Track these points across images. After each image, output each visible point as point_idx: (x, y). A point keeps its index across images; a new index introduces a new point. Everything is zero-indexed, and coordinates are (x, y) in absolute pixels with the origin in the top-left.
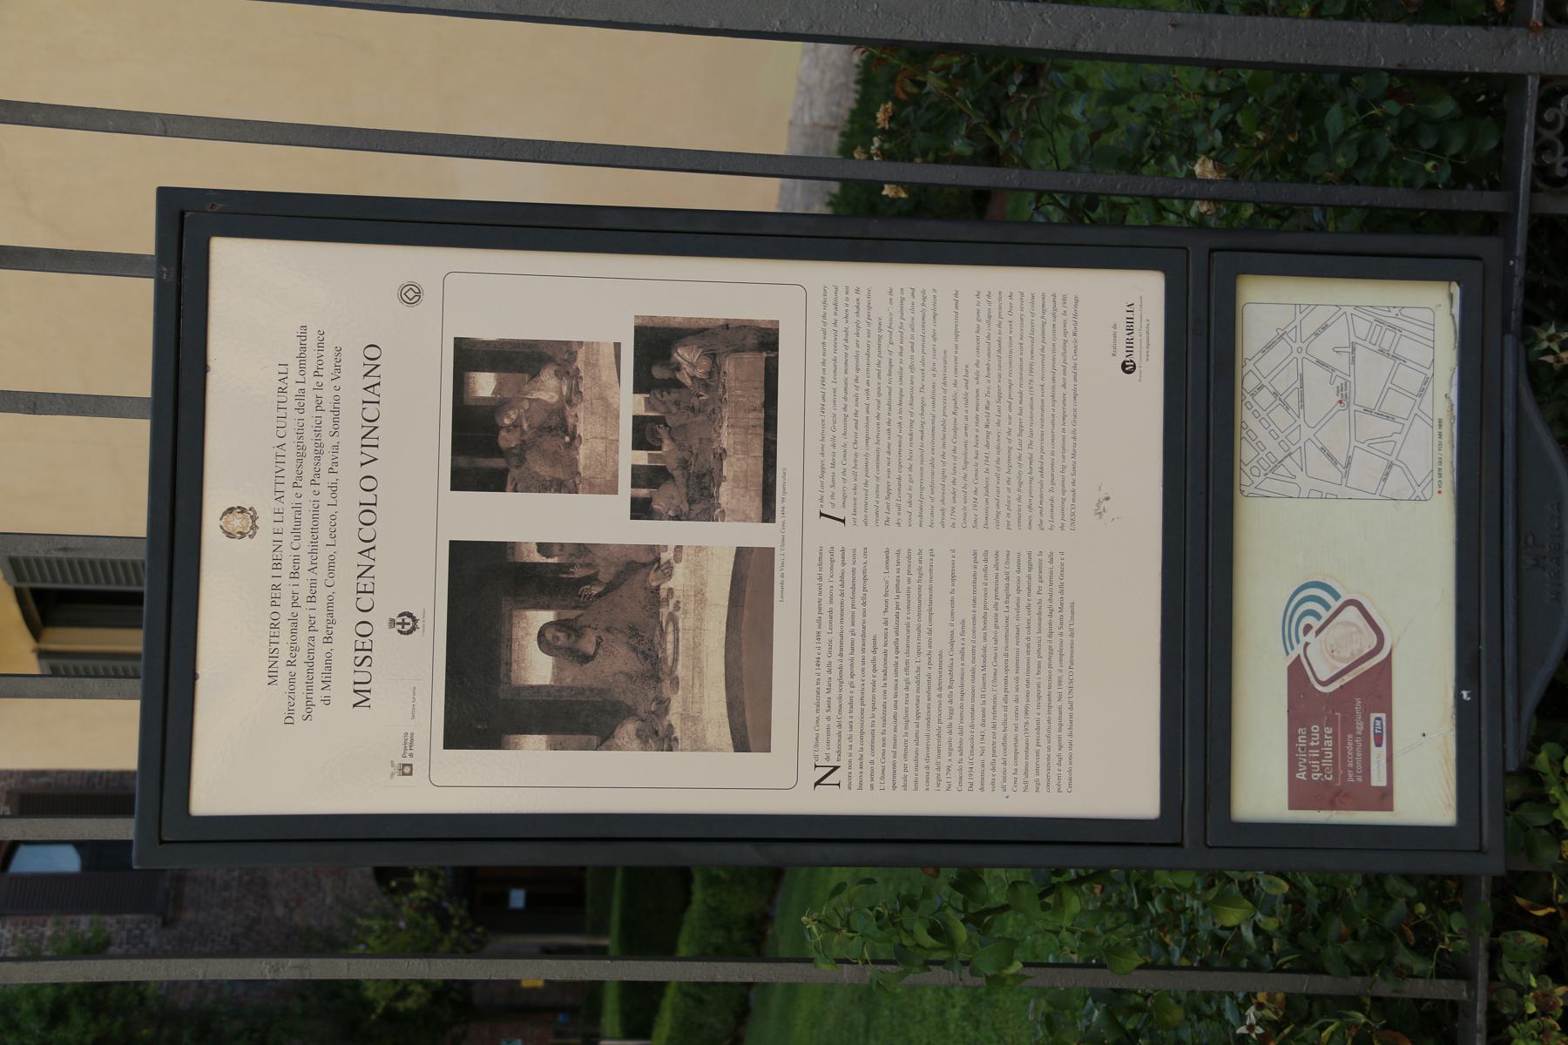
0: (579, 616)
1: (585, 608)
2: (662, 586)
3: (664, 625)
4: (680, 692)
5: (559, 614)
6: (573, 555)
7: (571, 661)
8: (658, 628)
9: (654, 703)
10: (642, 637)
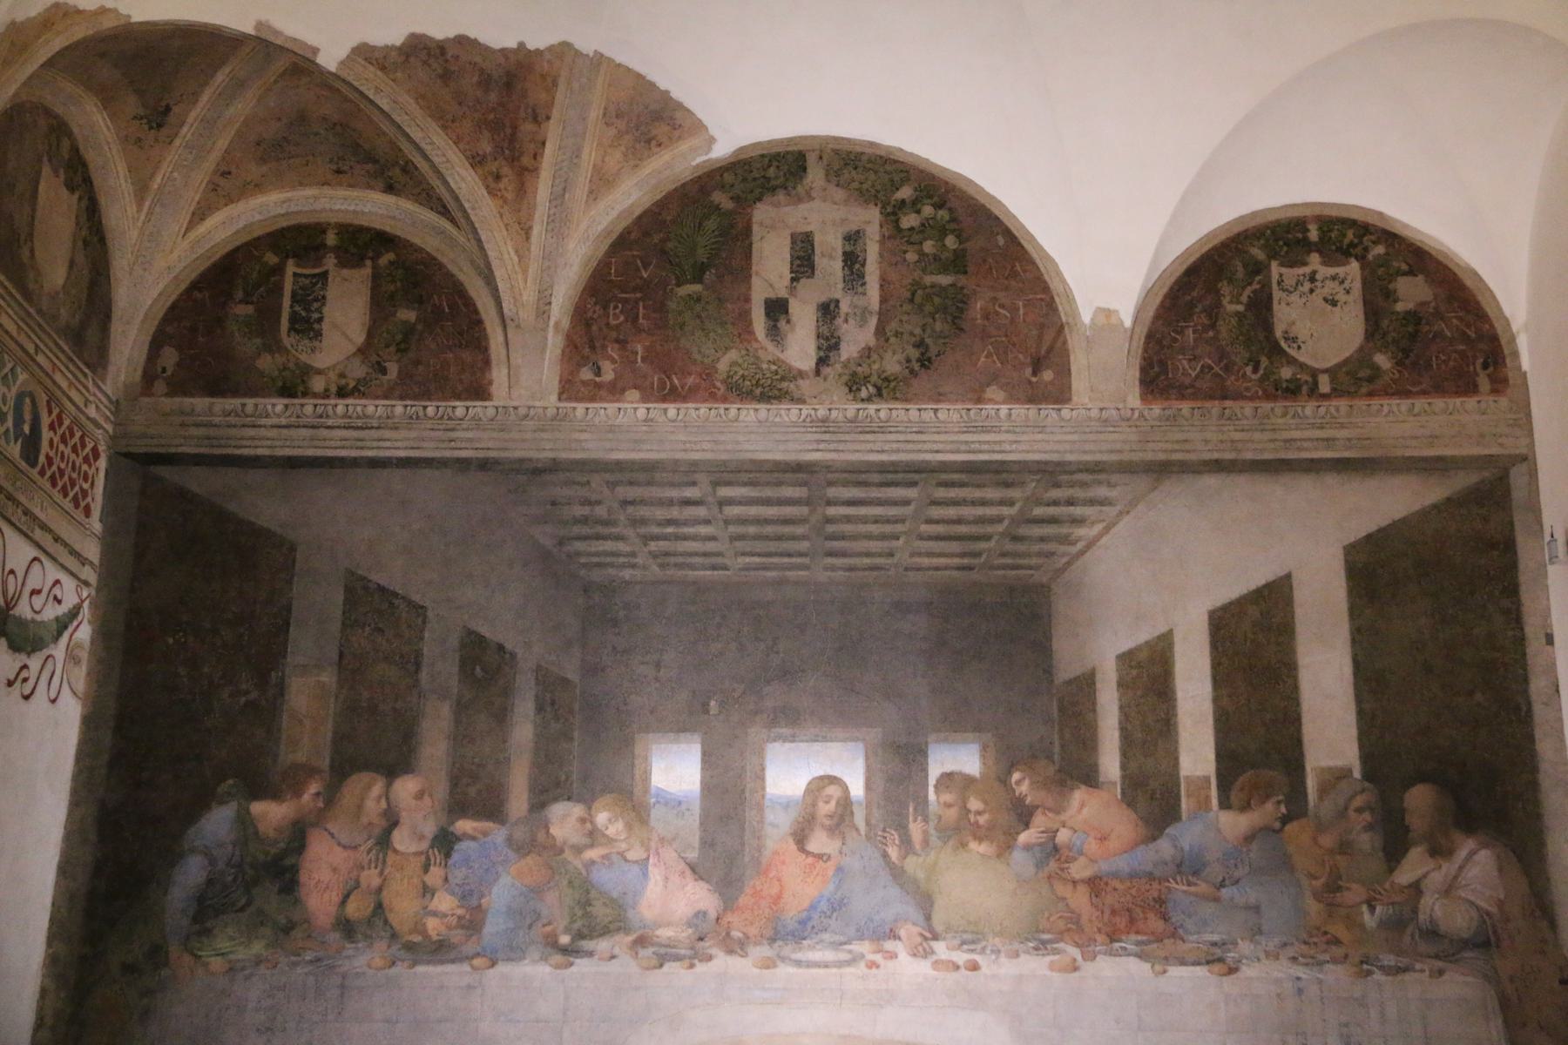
0: (857, 830)
1: (868, 838)
2: (897, 941)
3: (847, 947)
4: (756, 971)
5: (860, 803)
8: (842, 939)
9: (740, 935)
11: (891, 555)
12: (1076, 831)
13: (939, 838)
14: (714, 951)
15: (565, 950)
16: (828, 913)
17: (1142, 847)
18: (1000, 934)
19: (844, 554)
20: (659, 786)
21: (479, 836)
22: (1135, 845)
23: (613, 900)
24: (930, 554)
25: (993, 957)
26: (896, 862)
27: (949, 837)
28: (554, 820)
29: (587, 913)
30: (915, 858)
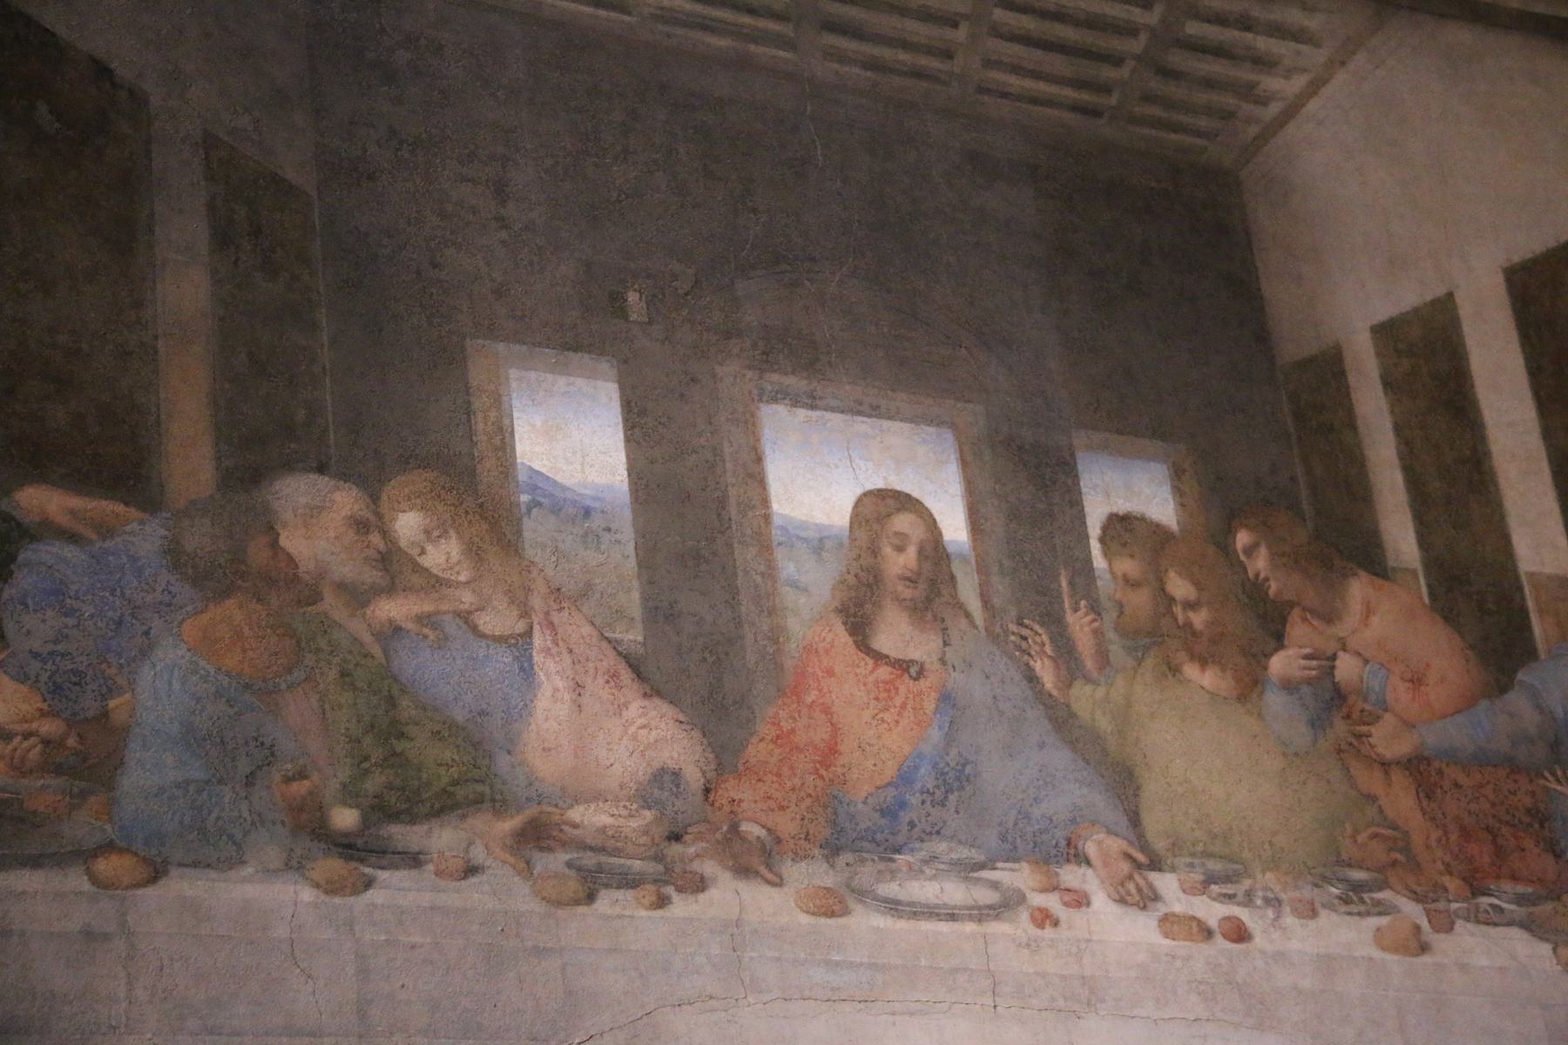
0: (968, 615)
2: (1084, 869)
3: (985, 874)
4: (805, 919)
5: (964, 559)
6: (1122, 613)
7: (843, 582)
8: (977, 856)
10: (943, 804)
11: (948, 55)
12: (1366, 661)
13: (1130, 650)
14: (709, 867)
15: (350, 847)
16: (939, 794)
17: (1484, 704)
18: (1273, 864)
19: (857, 33)
20: (537, 466)
21: (94, 537)
22: (1470, 702)
23: (453, 726)
24: (1016, 69)
25: (1270, 913)
26: (1055, 693)
27: (1147, 648)
28: (287, 515)
29: (395, 754)
30: (1088, 689)
